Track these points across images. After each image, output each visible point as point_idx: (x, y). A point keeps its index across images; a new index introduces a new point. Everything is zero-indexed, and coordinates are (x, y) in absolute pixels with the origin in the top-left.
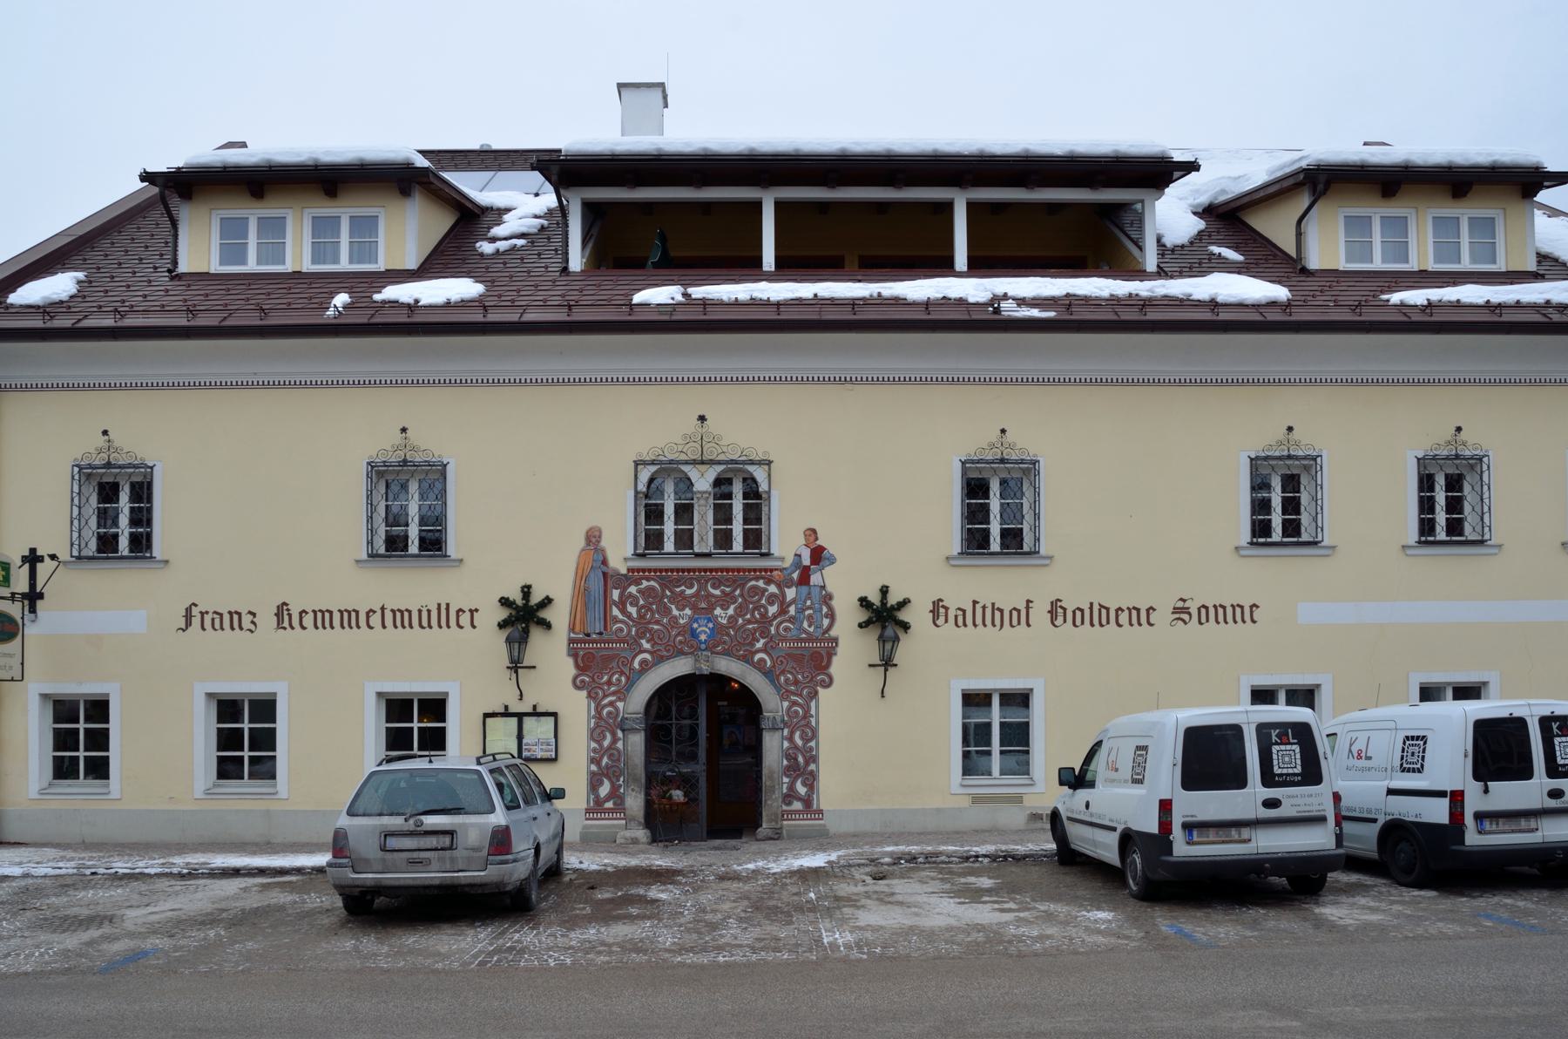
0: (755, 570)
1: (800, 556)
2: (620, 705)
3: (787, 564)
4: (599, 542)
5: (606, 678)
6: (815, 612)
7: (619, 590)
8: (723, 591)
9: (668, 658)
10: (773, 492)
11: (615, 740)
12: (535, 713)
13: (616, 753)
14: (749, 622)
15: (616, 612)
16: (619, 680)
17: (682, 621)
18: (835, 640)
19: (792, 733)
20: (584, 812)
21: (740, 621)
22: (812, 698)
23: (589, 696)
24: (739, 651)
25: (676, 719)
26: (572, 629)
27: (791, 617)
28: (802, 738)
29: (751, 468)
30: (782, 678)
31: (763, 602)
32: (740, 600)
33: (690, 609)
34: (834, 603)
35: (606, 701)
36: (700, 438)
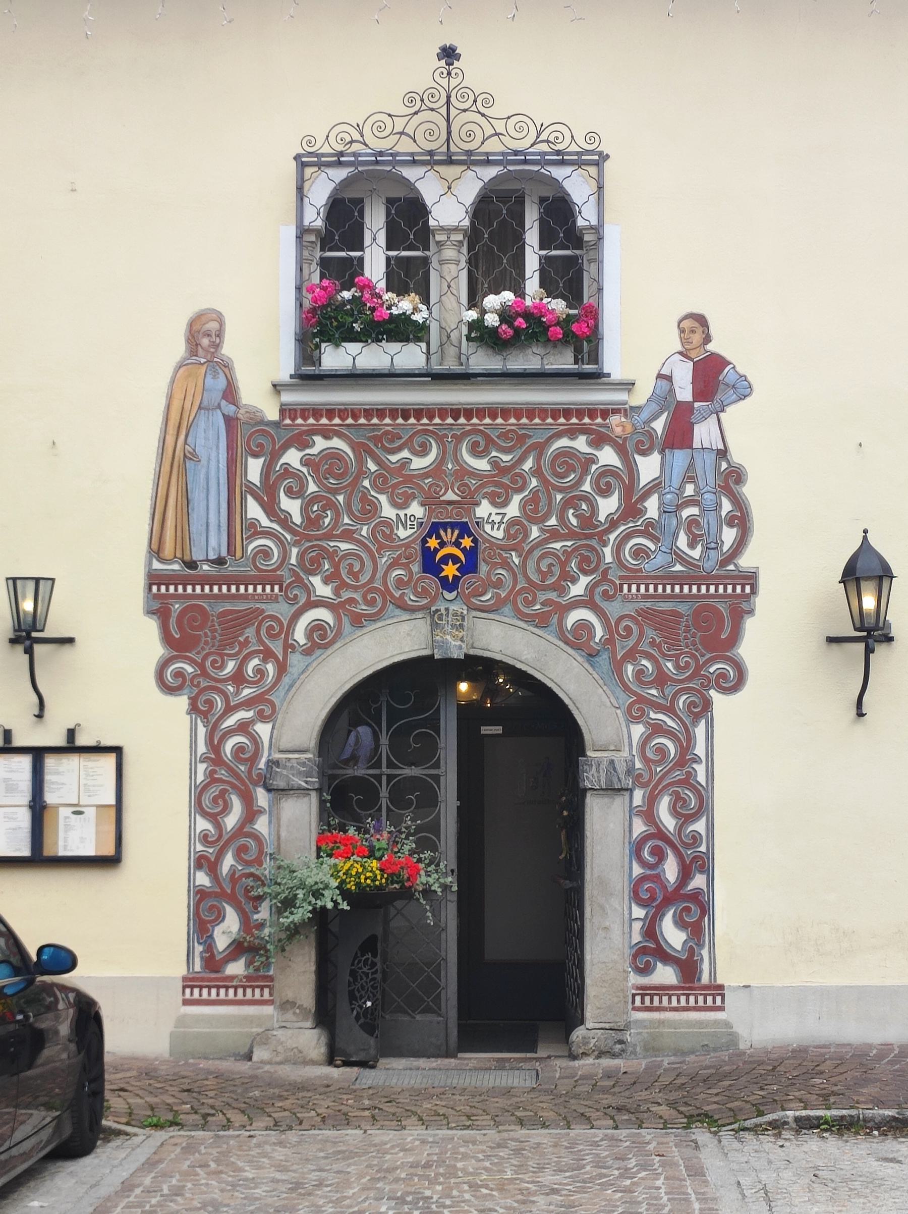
0: (567, 413)
1: (669, 378)
2: (263, 730)
3: (640, 396)
4: (217, 346)
5: (231, 666)
6: (703, 510)
7: (262, 459)
8: (495, 463)
9: (374, 618)
10: (610, 233)
11: (251, 814)
12: (71, 747)
13: (252, 843)
14: (554, 535)
15: (254, 510)
16: (260, 672)
17: (402, 533)
18: (751, 579)
19: (652, 800)
20: (180, 984)
21: (535, 532)
22: (696, 718)
23: (194, 708)
24: (533, 602)
25: (390, 765)
26: (156, 551)
27: (650, 524)
28: (674, 811)
29: (558, 173)
30: (630, 668)
31: (587, 487)
32: (534, 482)
33: (423, 505)
34: (748, 490)
35: (231, 721)
36: (444, 99)
